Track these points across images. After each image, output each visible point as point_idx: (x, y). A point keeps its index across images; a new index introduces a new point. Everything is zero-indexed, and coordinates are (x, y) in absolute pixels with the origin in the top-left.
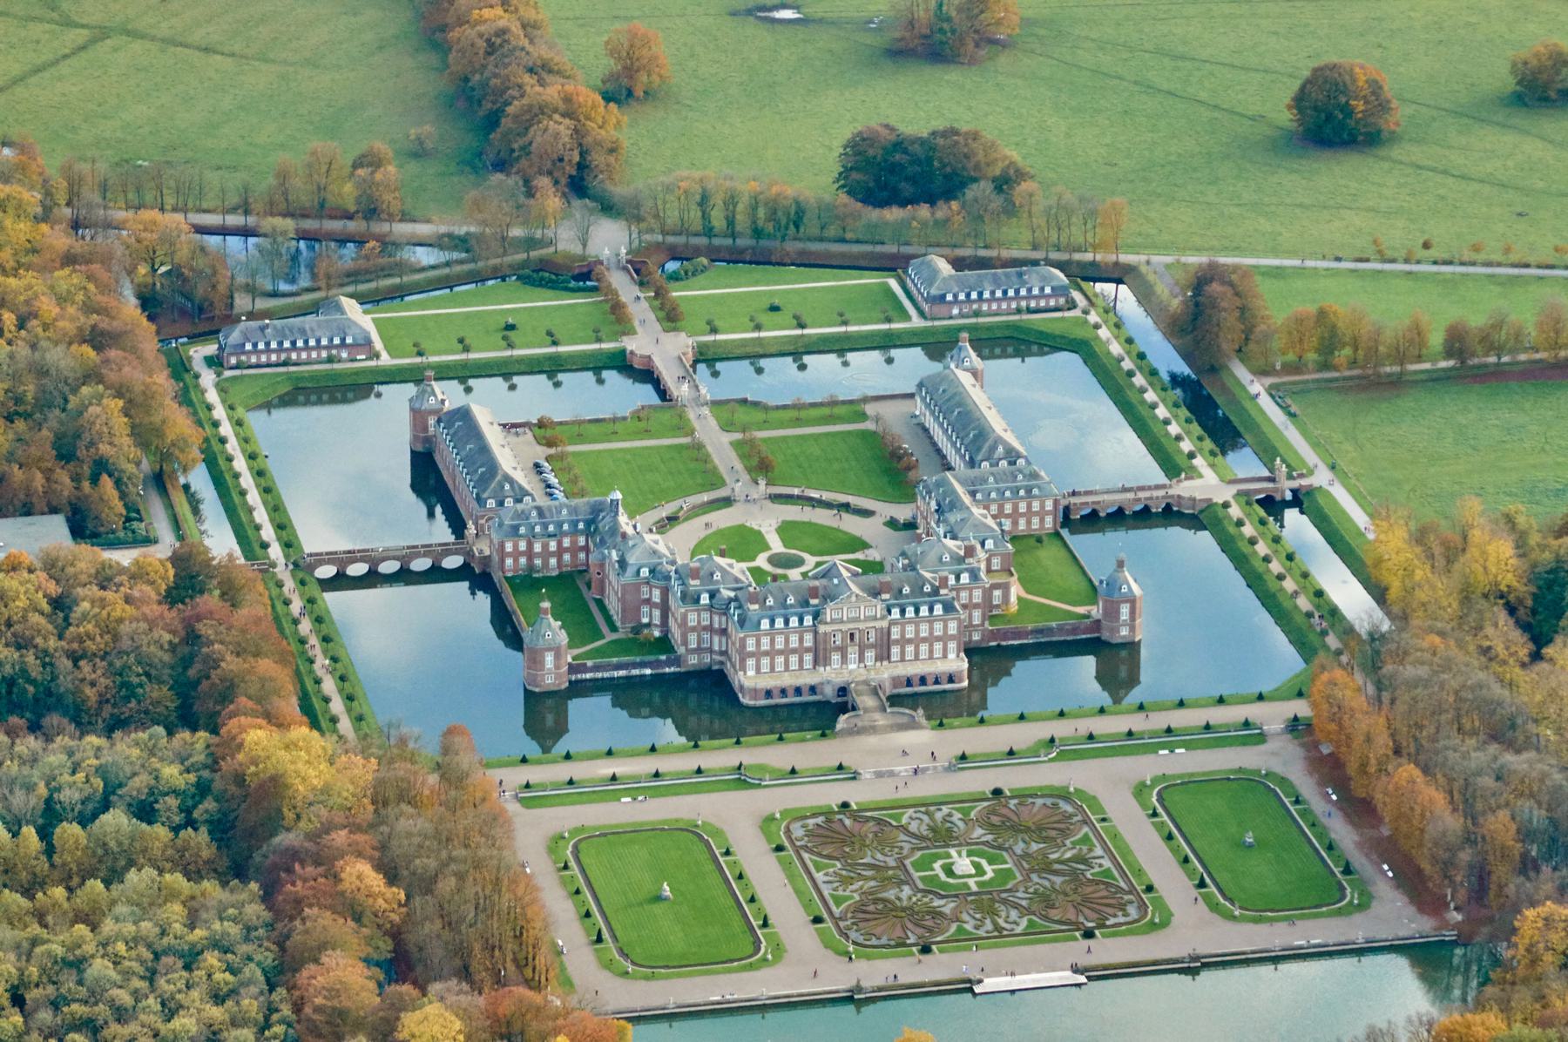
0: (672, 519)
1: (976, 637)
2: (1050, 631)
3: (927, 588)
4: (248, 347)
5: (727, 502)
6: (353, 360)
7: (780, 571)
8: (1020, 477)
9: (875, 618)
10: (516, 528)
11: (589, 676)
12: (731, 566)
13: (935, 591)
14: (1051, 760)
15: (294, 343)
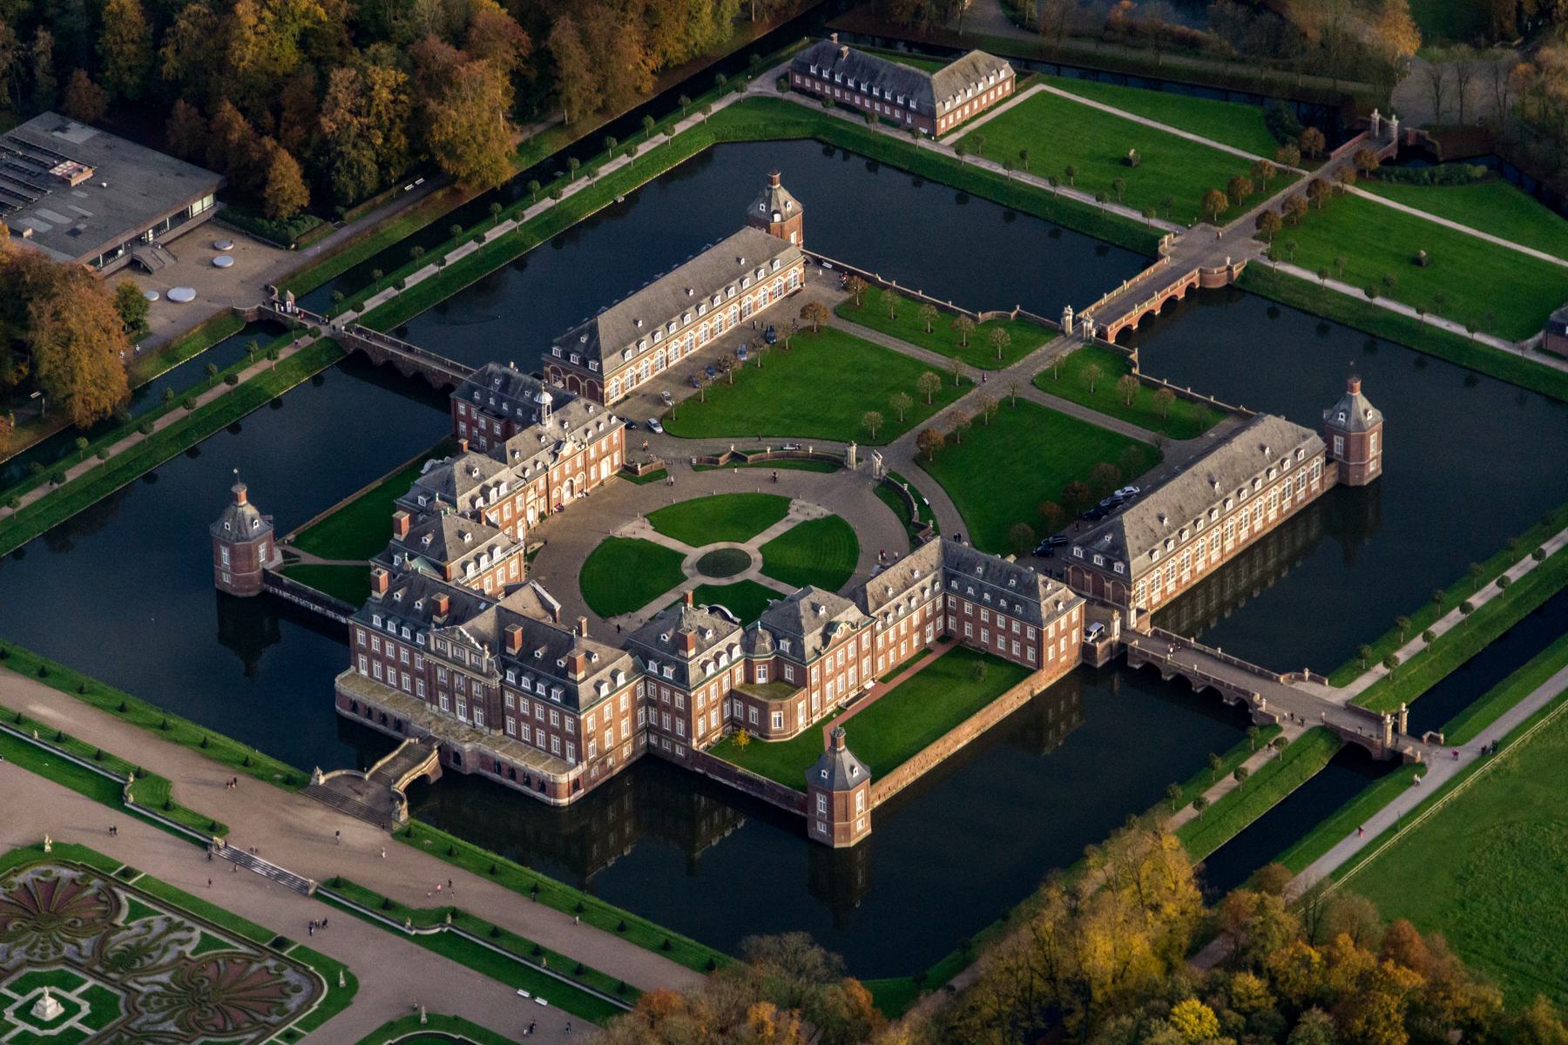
0: (738, 458)
1: (679, 751)
2: (759, 784)
3: (561, 663)
4: (813, 70)
5: (834, 464)
6: (912, 131)
7: (686, 572)
8: (1013, 582)
9: (479, 671)
10: (472, 389)
11: (286, 595)
12: (461, 535)
13: (563, 673)
14: (418, 939)
15: (858, 85)
